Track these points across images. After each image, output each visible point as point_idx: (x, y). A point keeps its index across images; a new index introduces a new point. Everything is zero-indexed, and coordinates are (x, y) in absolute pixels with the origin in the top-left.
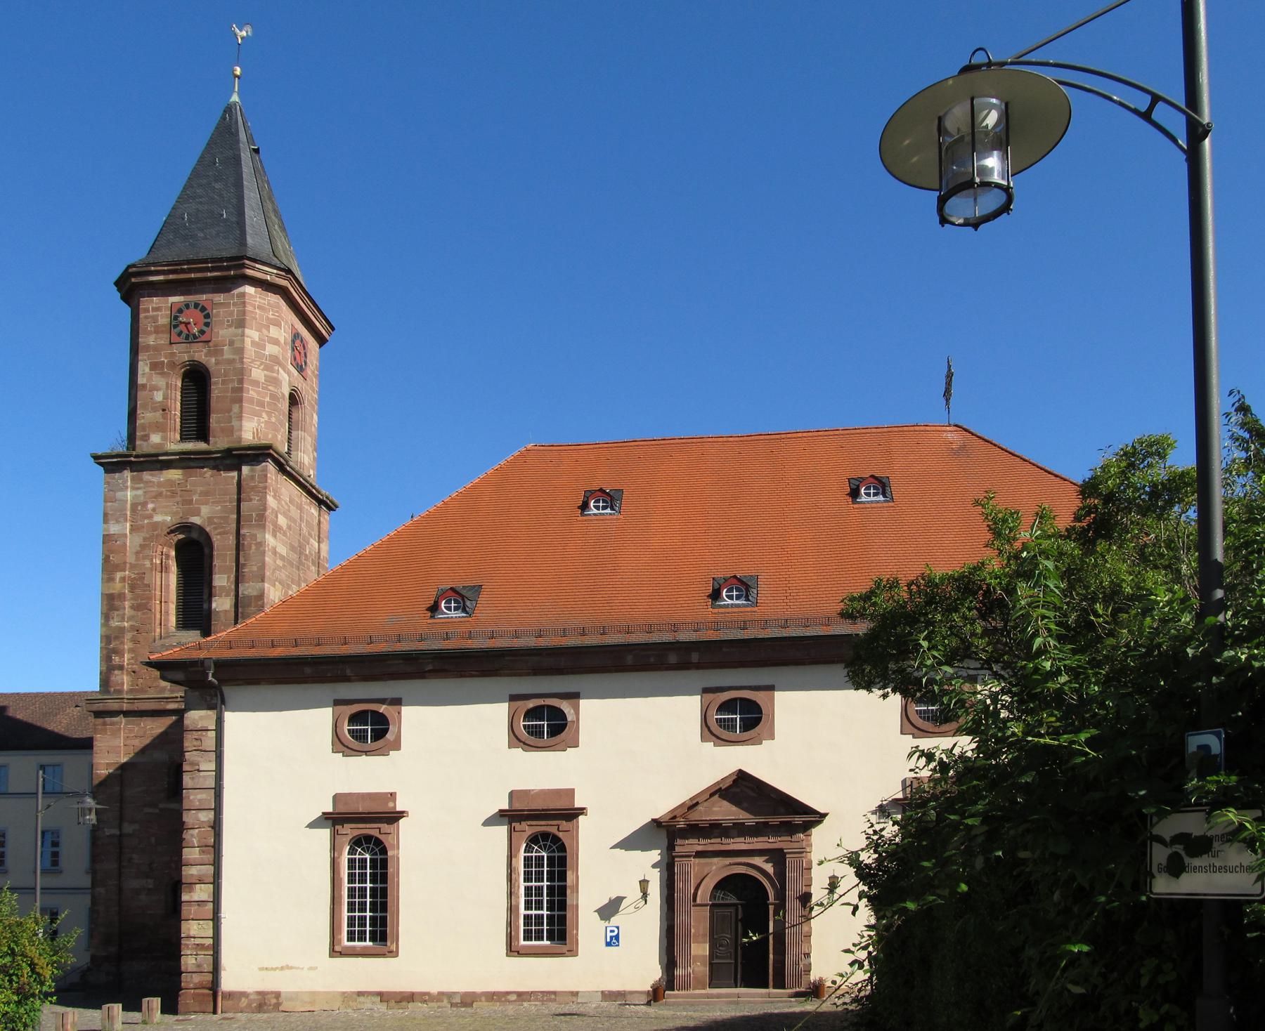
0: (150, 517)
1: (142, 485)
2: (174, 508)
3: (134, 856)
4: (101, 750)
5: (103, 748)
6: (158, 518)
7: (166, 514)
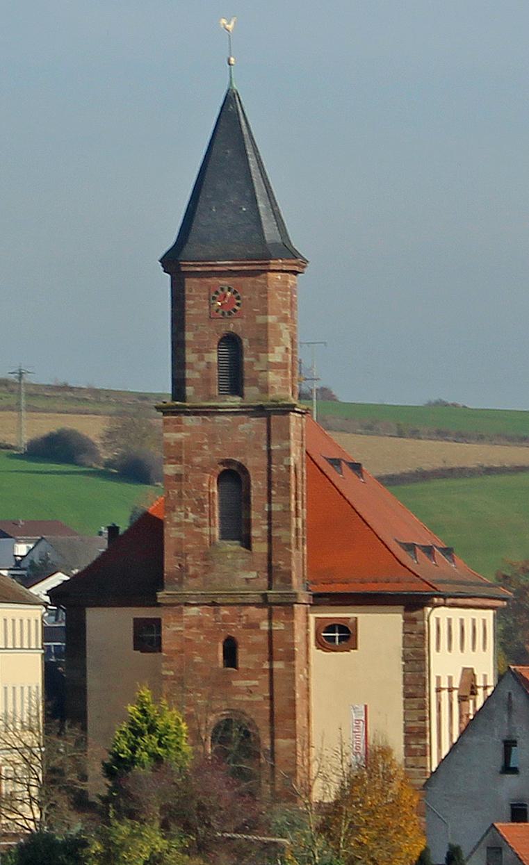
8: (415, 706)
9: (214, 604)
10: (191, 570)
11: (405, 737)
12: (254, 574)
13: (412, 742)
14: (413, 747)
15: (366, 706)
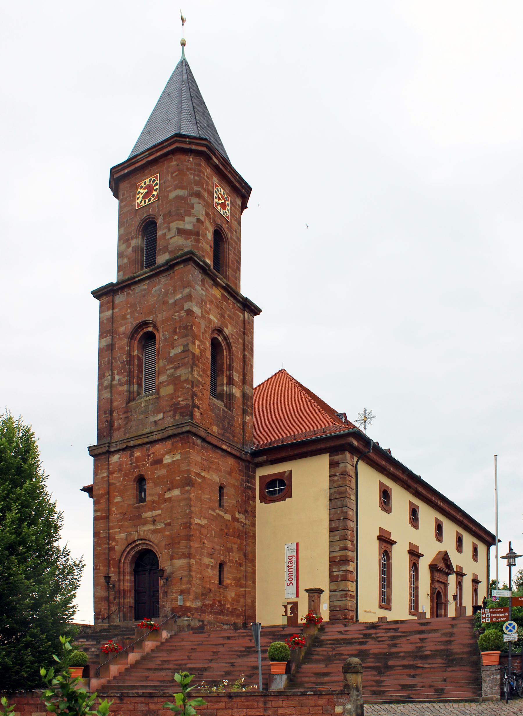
0: (209, 314)
1: (204, 289)
2: (219, 316)
3: (205, 541)
4: (192, 461)
5: (193, 460)
6: (211, 317)
7: (216, 317)
8: (337, 538)
9: (127, 448)
10: (116, 425)
11: (330, 565)
12: (161, 416)
13: (334, 570)
14: (335, 574)
15: (297, 544)
